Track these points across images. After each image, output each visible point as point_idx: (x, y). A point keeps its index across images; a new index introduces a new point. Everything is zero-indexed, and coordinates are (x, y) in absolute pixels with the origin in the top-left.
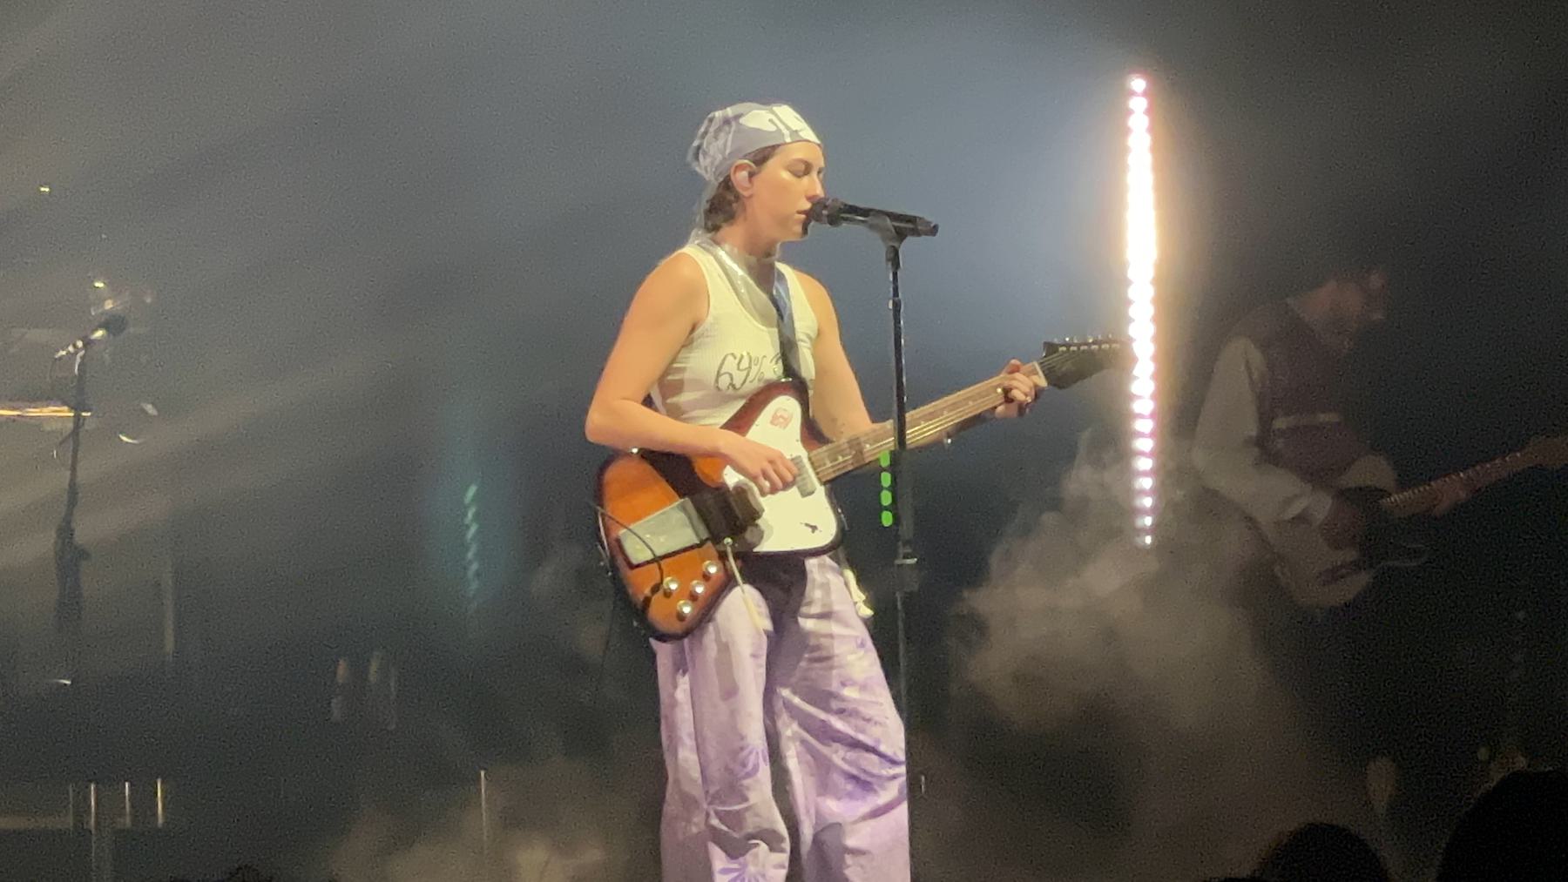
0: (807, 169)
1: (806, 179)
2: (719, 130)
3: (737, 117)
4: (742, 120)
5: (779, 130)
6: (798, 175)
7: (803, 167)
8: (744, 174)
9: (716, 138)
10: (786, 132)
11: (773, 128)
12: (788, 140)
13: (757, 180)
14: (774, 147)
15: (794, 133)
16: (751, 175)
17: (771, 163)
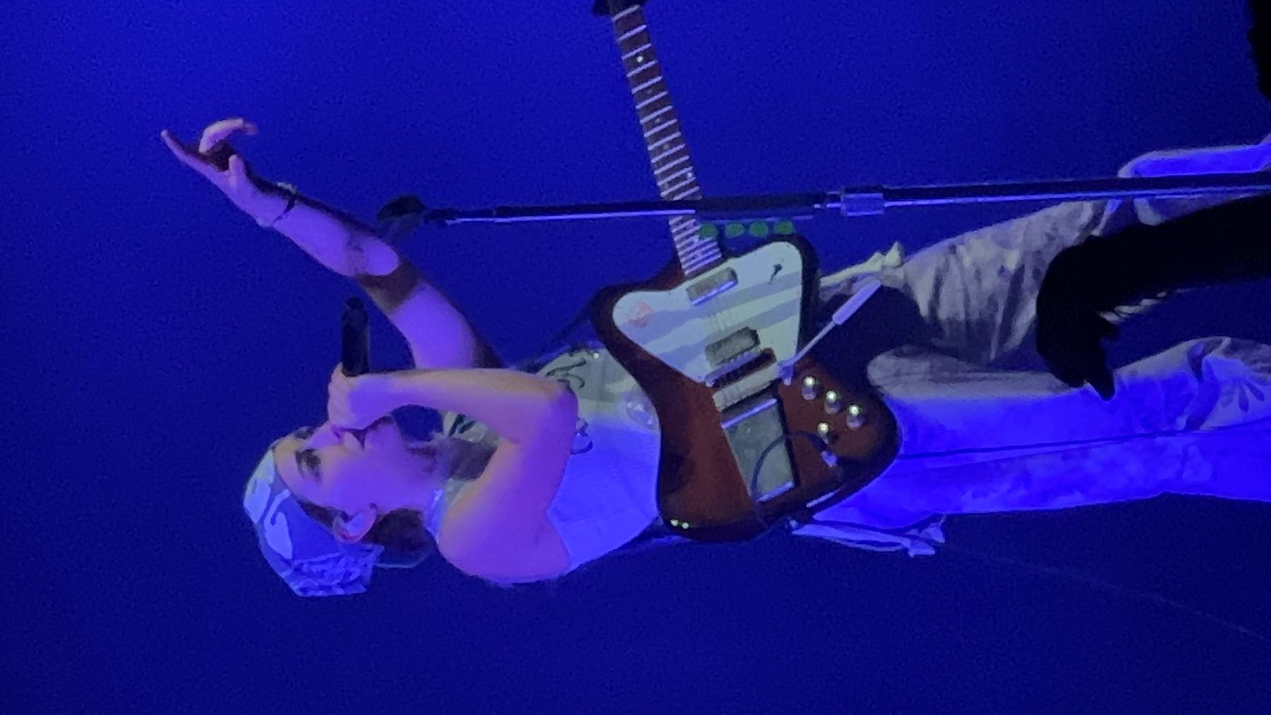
5: (281, 507)
11: (281, 516)
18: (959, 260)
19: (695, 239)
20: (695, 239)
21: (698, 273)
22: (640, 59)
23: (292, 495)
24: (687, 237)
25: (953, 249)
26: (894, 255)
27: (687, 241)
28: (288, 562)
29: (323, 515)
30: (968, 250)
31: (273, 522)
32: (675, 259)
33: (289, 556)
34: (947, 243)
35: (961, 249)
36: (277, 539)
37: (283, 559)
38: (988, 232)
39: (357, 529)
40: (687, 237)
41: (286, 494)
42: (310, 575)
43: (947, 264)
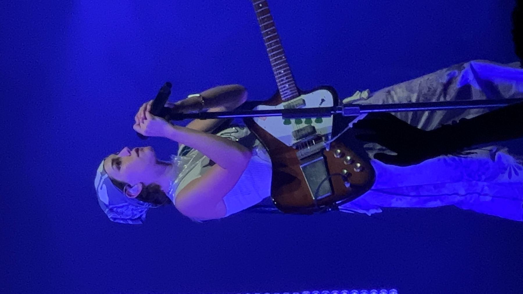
2: (117, 212)
4: (107, 203)
9: (122, 213)
19: (287, 86)
21: (288, 100)
22: (261, 5)
23: (109, 177)
24: (283, 84)
25: (389, 92)
26: (365, 94)
27: (283, 86)
28: (107, 206)
33: (107, 203)
35: (393, 93)
37: (105, 204)
40: (283, 84)
41: (106, 176)
42: (117, 212)
43: (387, 99)
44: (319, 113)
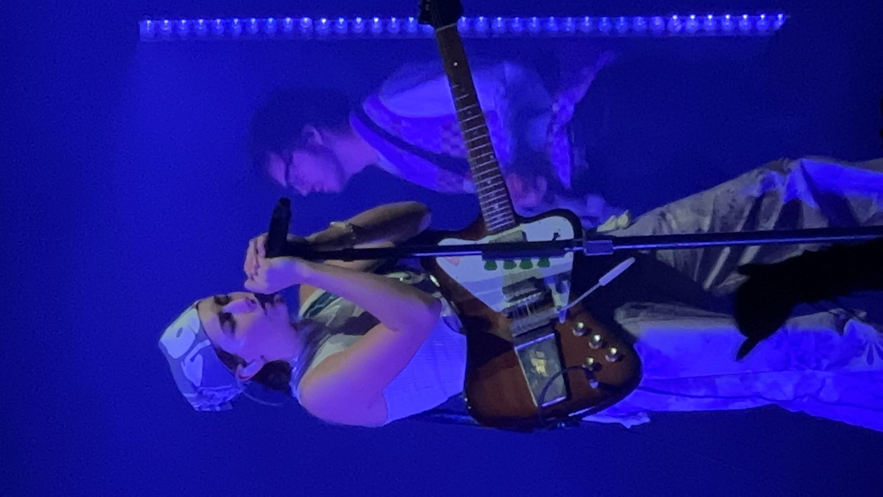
0: (225, 318)
1: (237, 317)
3: (195, 388)
4: (198, 384)
5: (199, 352)
6: (233, 325)
7: (227, 323)
8: (246, 370)
10: (200, 346)
11: (199, 358)
12: (208, 343)
13: (247, 361)
14: (216, 350)
15: (198, 339)
16: (245, 365)
17: (231, 349)
18: (669, 226)
20: (496, 206)
21: (497, 232)
24: (490, 203)
25: (663, 215)
26: (624, 219)
29: (229, 360)
30: (675, 218)
31: (192, 360)
32: (481, 215)
34: (658, 210)
35: (669, 216)
36: (192, 372)
38: (687, 201)
39: (248, 373)
40: (490, 203)
43: (660, 224)
44: (555, 247)
